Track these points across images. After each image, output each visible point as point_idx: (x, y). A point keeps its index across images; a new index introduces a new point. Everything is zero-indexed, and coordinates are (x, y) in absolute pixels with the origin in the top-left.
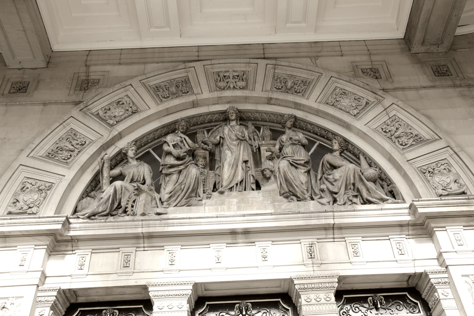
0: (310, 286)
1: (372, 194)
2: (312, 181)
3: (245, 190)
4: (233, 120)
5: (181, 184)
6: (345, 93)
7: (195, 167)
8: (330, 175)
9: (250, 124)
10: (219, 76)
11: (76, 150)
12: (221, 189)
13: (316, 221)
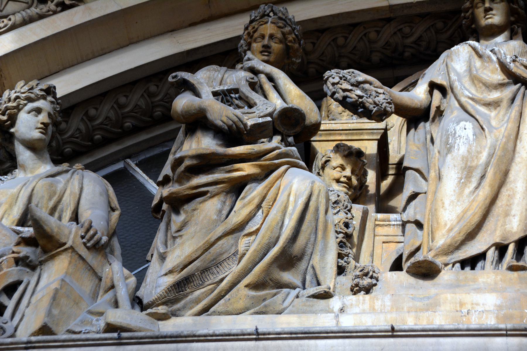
4: (492, 32)
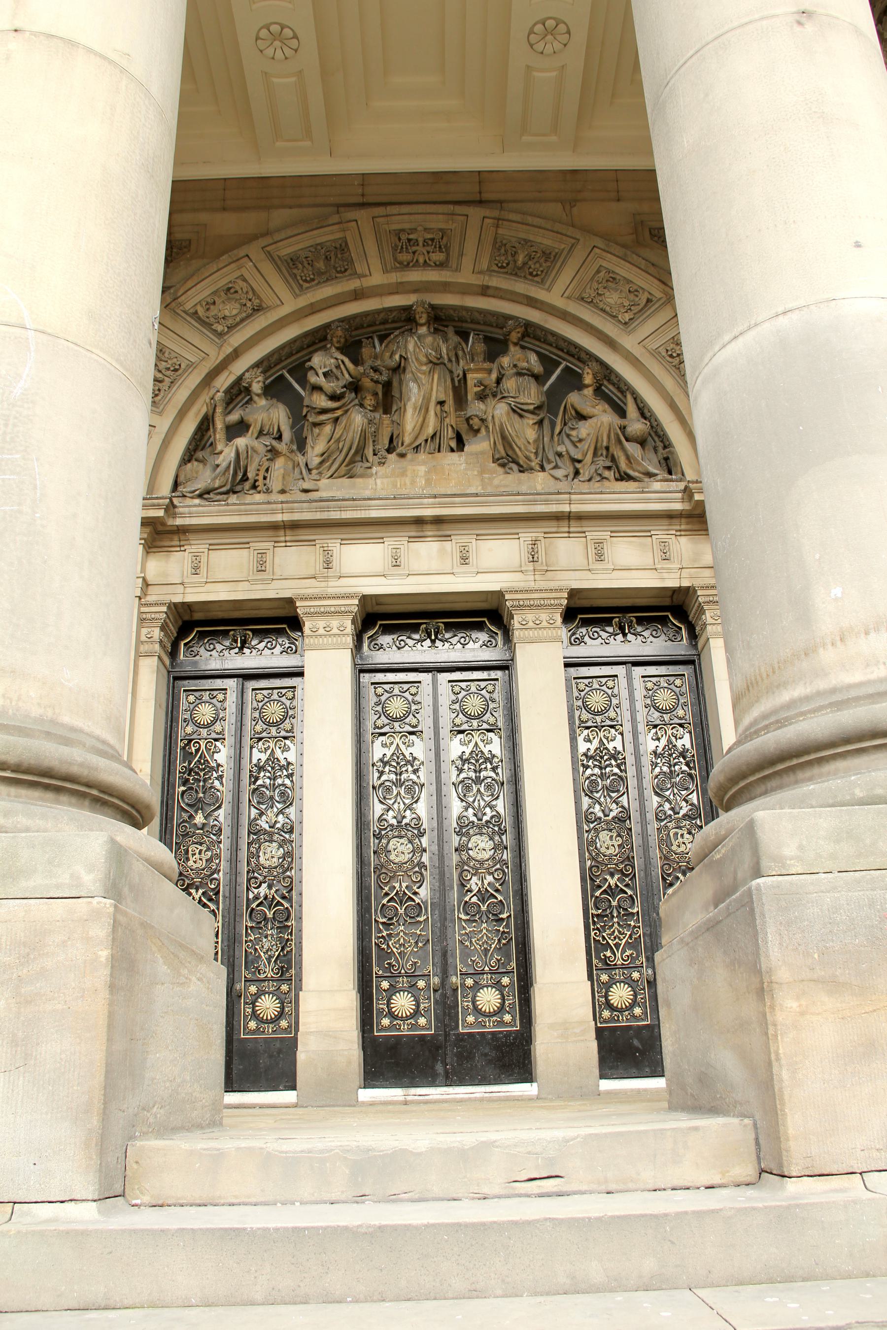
0: (527, 603)
1: (634, 465)
2: (545, 439)
3: (439, 451)
4: (422, 325)
5: (338, 441)
6: (614, 279)
7: (361, 412)
8: (573, 429)
9: (450, 331)
10: (400, 239)
11: (166, 379)
12: (400, 450)
13: (543, 506)
